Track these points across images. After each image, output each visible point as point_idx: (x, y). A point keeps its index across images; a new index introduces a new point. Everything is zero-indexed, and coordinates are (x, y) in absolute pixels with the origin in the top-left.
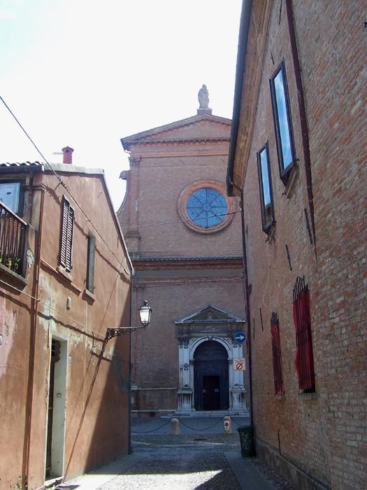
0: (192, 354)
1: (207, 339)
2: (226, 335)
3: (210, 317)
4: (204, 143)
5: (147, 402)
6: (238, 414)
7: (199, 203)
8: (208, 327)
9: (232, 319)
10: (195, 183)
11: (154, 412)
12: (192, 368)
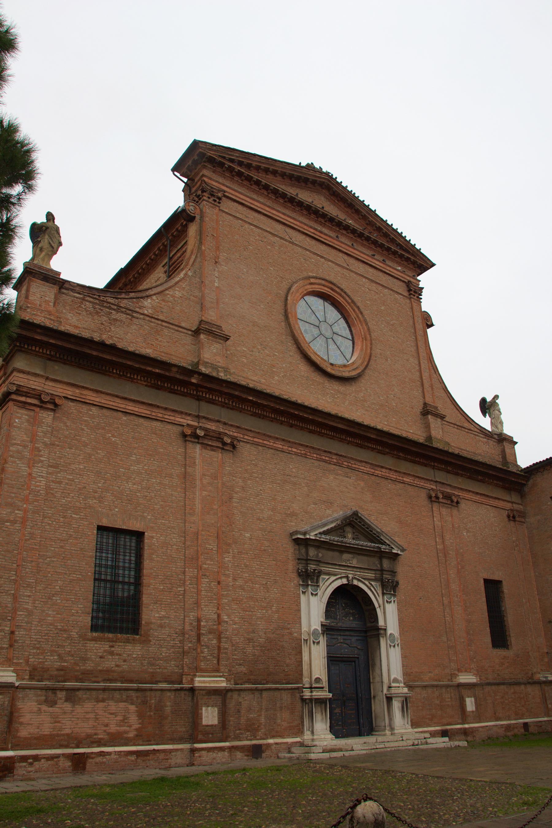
0: (323, 606)
1: (345, 581)
2: (371, 575)
3: (350, 536)
4: (323, 221)
5: (243, 721)
6: (427, 743)
7: (313, 317)
8: (346, 556)
9: (384, 543)
10: (312, 280)
11: (260, 746)
12: (323, 641)
